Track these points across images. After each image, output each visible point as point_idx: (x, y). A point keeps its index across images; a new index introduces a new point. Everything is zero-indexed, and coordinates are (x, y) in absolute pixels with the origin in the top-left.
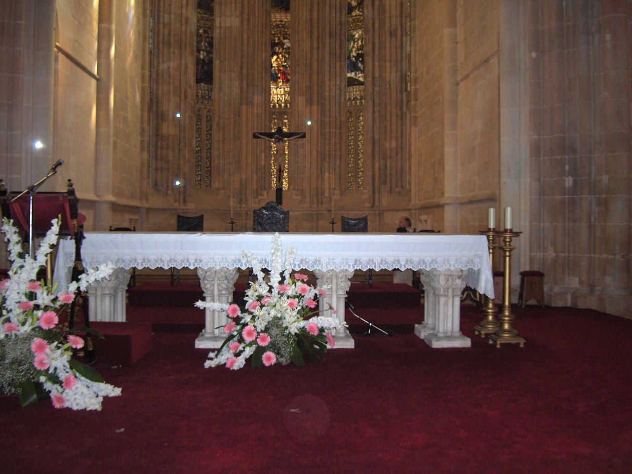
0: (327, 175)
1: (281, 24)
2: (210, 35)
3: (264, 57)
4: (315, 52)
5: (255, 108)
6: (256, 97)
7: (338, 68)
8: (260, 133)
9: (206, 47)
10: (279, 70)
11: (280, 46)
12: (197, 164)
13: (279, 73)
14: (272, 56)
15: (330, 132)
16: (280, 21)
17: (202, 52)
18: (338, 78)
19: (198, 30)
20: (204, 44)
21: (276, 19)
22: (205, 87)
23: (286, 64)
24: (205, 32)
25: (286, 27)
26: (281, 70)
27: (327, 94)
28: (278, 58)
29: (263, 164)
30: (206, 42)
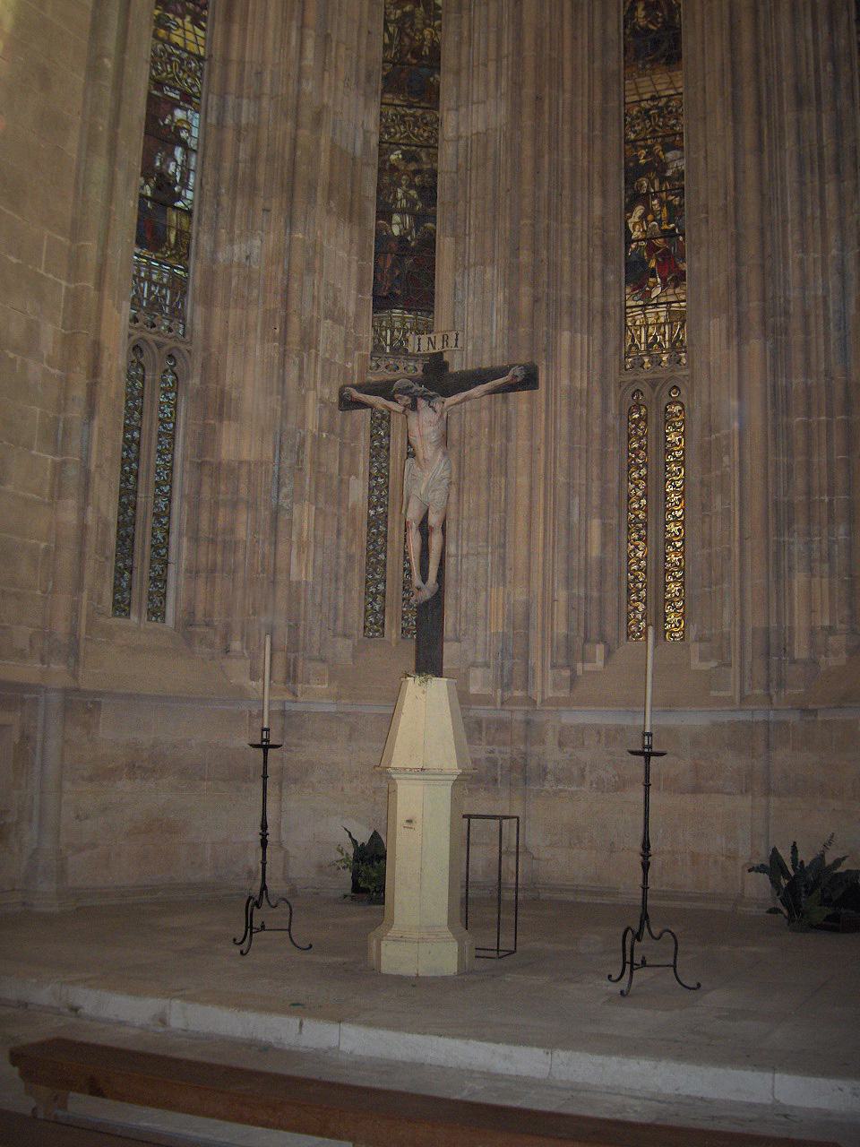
0: (799, 579)
1: (657, 107)
2: (425, 167)
3: (597, 211)
4: (749, 161)
5: (564, 371)
6: (566, 335)
7: (831, 203)
8: (359, 388)
9: (412, 202)
10: (652, 249)
11: (652, 175)
12: (373, 560)
13: (650, 256)
14: (629, 209)
15: (807, 425)
16: (653, 98)
17: (396, 218)
18: (833, 237)
19: (383, 151)
20: (405, 193)
21: (639, 94)
22: (403, 319)
23: (672, 225)
24: (409, 157)
25: (671, 112)
26: (659, 249)
27: (794, 294)
28: (648, 210)
29: (595, 551)
30: (411, 186)
